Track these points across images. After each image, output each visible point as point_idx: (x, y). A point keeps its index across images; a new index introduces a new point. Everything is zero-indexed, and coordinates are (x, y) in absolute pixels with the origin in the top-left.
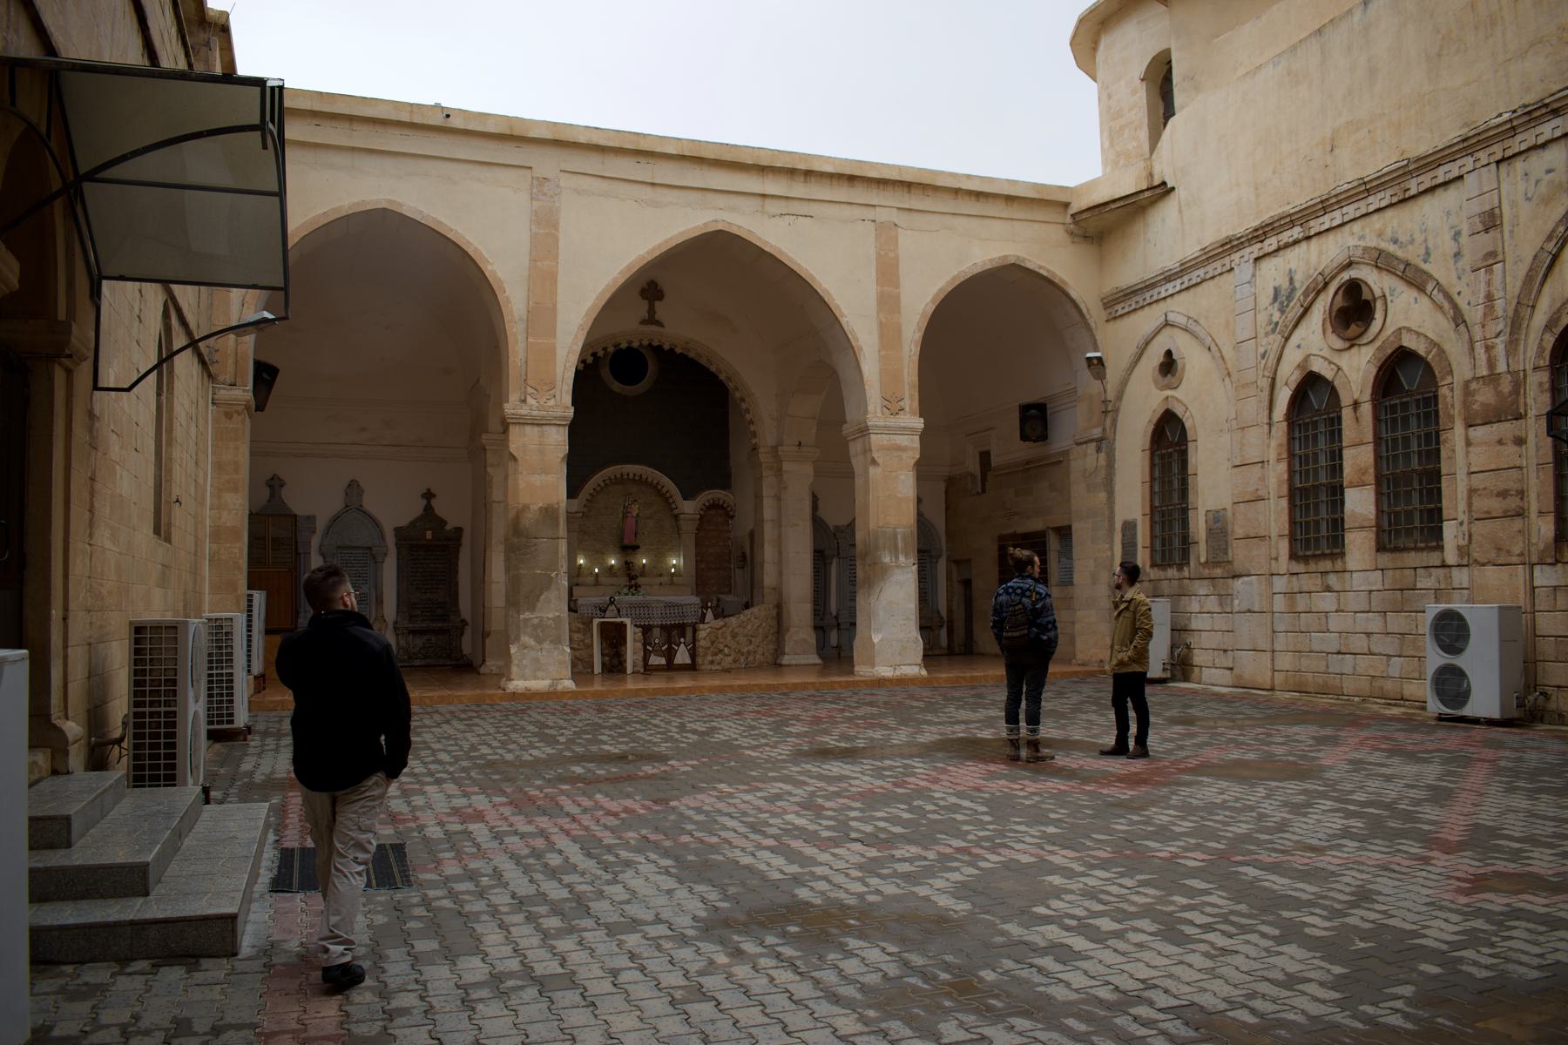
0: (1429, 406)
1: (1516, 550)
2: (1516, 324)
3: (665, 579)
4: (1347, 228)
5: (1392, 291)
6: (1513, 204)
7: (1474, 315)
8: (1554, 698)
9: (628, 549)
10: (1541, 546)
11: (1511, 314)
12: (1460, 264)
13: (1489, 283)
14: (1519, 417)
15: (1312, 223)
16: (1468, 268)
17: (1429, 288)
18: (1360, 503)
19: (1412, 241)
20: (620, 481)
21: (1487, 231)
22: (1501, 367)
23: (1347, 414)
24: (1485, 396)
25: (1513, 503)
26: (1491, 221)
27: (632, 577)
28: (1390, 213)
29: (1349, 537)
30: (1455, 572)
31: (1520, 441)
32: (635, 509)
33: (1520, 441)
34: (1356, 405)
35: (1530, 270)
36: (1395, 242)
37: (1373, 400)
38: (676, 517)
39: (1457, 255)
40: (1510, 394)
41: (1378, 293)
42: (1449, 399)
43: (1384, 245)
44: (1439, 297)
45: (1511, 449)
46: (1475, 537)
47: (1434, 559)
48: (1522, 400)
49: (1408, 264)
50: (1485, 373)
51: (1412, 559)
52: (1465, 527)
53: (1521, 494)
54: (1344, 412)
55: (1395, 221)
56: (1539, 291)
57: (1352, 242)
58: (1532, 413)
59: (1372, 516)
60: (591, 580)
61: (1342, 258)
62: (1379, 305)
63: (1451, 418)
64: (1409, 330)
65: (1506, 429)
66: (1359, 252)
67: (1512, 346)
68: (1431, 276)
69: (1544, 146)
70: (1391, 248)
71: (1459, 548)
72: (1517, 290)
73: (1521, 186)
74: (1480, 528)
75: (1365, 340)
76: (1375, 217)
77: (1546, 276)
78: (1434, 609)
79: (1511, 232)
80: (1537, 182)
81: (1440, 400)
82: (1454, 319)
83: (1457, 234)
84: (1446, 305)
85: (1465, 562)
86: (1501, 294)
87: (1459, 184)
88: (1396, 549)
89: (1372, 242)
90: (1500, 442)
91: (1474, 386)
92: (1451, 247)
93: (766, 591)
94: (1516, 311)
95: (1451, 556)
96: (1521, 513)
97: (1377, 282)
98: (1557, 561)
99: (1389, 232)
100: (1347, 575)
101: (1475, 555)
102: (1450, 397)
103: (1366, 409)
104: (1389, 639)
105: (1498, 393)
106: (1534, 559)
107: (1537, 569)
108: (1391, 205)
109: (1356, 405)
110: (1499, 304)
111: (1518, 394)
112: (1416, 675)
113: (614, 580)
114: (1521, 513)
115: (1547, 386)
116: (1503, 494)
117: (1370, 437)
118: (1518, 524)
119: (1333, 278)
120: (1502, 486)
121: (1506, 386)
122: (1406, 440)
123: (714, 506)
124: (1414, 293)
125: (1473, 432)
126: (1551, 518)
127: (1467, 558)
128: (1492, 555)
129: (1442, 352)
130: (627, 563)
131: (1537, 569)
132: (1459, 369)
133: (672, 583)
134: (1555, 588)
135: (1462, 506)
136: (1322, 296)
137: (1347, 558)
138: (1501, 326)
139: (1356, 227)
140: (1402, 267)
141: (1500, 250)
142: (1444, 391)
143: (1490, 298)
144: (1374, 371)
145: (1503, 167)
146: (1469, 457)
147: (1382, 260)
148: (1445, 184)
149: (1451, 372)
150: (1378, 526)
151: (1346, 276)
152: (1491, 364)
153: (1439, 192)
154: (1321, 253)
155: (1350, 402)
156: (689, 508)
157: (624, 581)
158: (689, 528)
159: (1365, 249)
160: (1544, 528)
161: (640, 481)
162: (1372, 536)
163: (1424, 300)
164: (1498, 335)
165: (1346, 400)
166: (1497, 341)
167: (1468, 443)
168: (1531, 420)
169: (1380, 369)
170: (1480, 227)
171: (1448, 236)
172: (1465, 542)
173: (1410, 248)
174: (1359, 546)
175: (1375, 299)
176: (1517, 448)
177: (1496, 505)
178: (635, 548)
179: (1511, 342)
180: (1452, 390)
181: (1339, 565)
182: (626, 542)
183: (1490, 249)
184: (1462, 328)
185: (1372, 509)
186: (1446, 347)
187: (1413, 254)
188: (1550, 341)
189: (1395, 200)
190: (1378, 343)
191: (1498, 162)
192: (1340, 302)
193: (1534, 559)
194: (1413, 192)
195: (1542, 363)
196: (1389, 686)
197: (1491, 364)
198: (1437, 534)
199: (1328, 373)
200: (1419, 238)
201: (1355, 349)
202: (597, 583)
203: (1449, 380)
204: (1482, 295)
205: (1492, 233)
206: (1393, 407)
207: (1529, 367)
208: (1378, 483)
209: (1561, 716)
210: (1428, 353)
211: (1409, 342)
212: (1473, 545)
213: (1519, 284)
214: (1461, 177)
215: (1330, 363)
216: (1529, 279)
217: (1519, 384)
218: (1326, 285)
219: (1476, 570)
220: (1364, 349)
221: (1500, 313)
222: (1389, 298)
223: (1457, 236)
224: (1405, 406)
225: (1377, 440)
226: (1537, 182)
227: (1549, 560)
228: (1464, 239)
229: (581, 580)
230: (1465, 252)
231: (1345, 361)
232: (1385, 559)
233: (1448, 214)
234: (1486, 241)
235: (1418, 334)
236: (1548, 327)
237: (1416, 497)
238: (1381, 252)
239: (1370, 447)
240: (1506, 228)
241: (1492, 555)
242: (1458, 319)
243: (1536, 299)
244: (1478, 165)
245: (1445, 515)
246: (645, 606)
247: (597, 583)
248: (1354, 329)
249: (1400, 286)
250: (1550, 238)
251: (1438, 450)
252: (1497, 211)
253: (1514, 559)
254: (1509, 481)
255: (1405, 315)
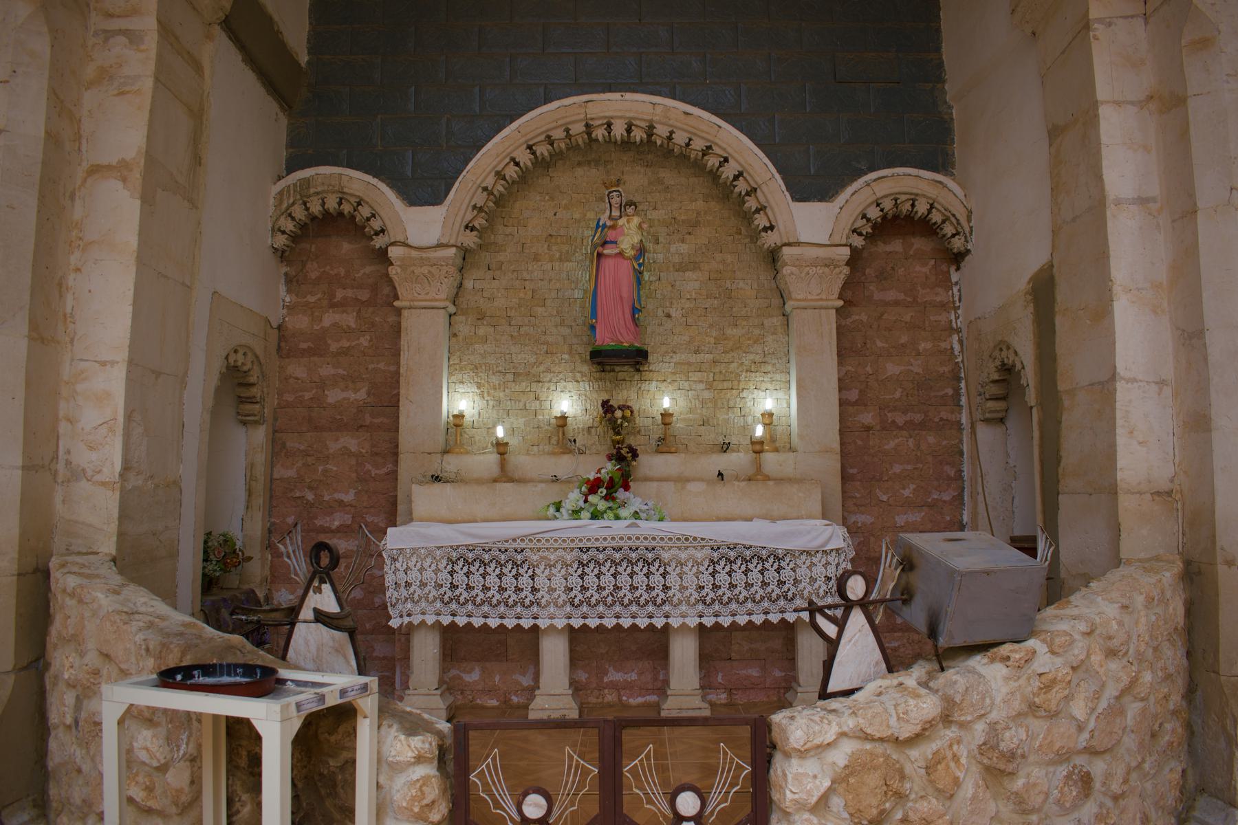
3: (737, 460)
9: (617, 361)
20: (589, 148)
27: (619, 461)
32: (629, 236)
38: (773, 257)
60: (492, 458)
93: (1126, 503)
113: (564, 465)
123: (896, 224)
130: (607, 407)
133: (757, 475)
156: (815, 227)
157: (599, 466)
158: (815, 292)
161: (649, 148)
178: (637, 358)
182: (604, 339)
202: (505, 475)
229: (452, 464)
246: (646, 558)
247: (505, 475)
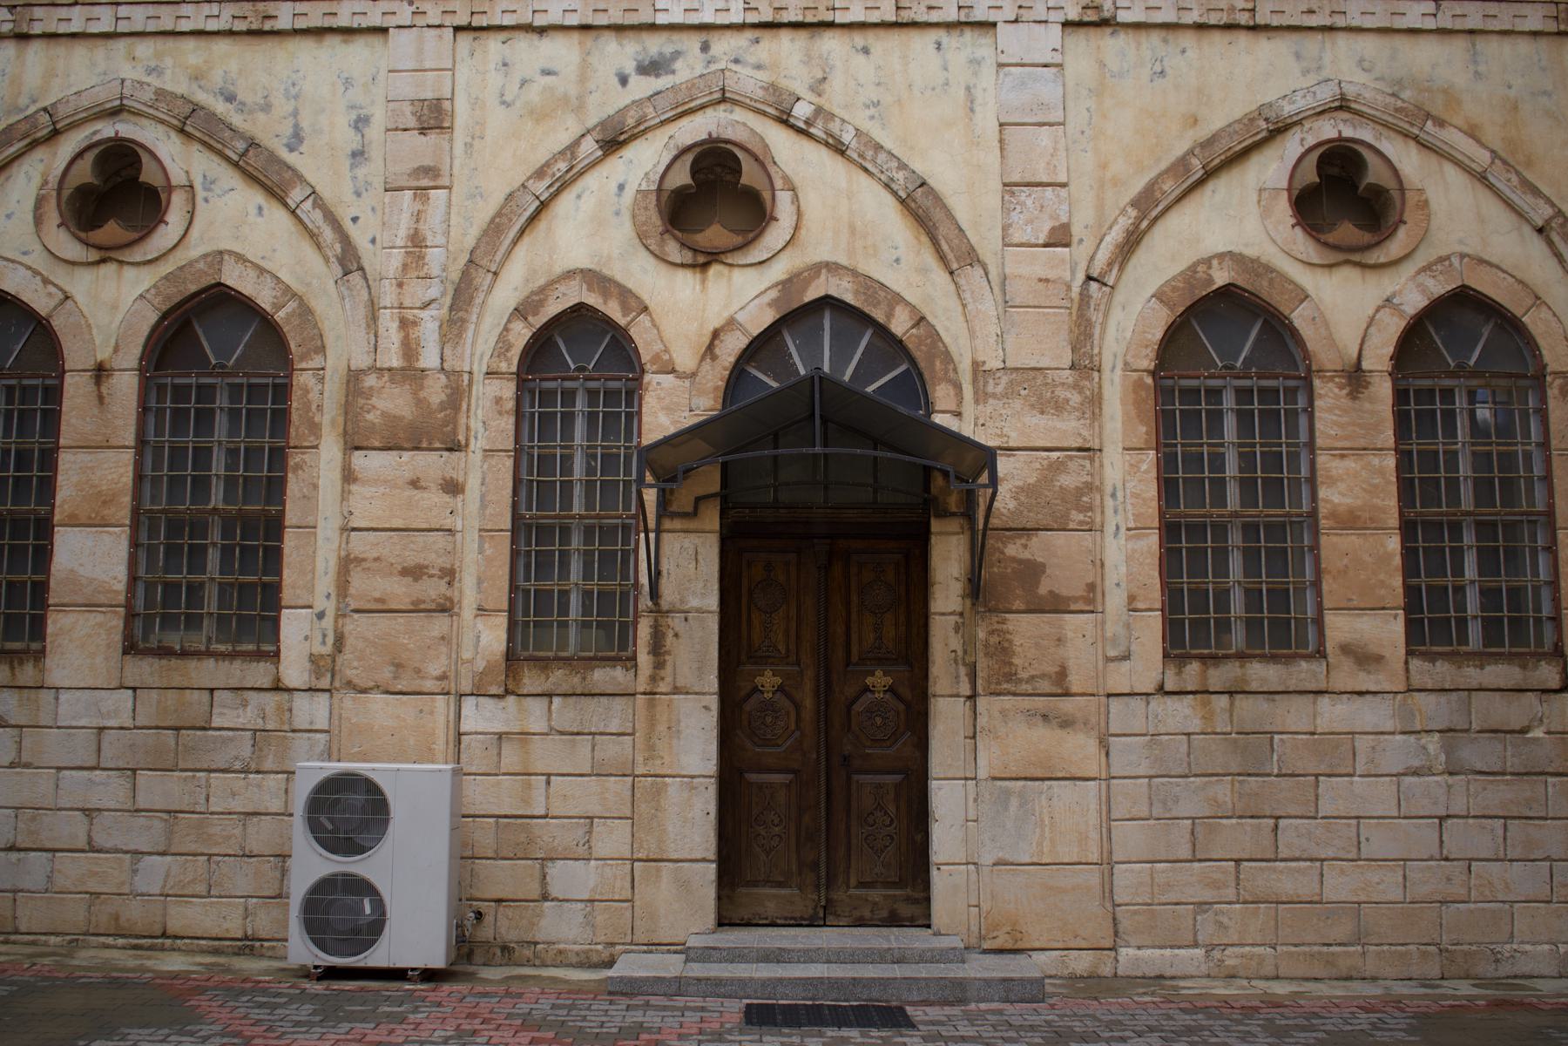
0: (269, 404)
1: (435, 669)
2: (463, 295)
4: (121, 44)
5: (209, 184)
6: (476, 103)
7: (384, 261)
8: (489, 919)
10: (480, 665)
11: (455, 276)
12: (361, 172)
13: (418, 217)
14: (454, 447)
15: (38, 12)
16: (378, 183)
17: (295, 195)
18: (91, 557)
19: (267, 107)
21: (423, 131)
22: (429, 358)
23: (76, 388)
24: (391, 402)
25: (432, 589)
26: (433, 118)
28: (222, 46)
29: (56, 623)
30: (300, 701)
31: (453, 488)
33: (453, 488)
34: (101, 372)
35: (499, 214)
36: (230, 98)
37: (141, 370)
39: (358, 155)
40: (443, 407)
41: (177, 177)
42: (314, 396)
43: (201, 97)
44: (315, 218)
45: (435, 498)
46: (350, 642)
47: (259, 673)
48: (462, 421)
49: (253, 144)
50: (396, 362)
51: (207, 672)
52: (328, 622)
53: (450, 575)
54: (69, 379)
55: (228, 60)
56: (509, 252)
57: (129, 72)
58: (477, 445)
59: (120, 586)
61: (106, 95)
62: (178, 201)
63: (315, 428)
64: (240, 258)
65: (431, 464)
66: (148, 96)
67: (453, 327)
68: (301, 178)
69: (542, 31)
70: (220, 107)
71: (314, 659)
72: (470, 242)
73: (495, 80)
74: (358, 627)
75: (137, 254)
76: (190, 44)
77: (522, 232)
78: (313, 770)
79: (469, 146)
80: (524, 83)
81: (296, 394)
82: (342, 261)
83: (360, 123)
84: (328, 234)
85: (325, 683)
86: (440, 240)
87: (376, 40)
88: (164, 652)
89: (176, 83)
90: (415, 484)
91: (370, 381)
92: (350, 140)
94: (465, 274)
95: (294, 670)
96: (446, 608)
97: (172, 155)
98: (508, 692)
99: (217, 78)
100: (46, 696)
101: (350, 673)
102: (318, 391)
103: (125, 385)
104: (141, 821)
105: (419, 402)
106: (466, 686)
107: (469, 704)
108: (231, 33)
109: (101, 372)
110: (435, 257)
111: (457, 409)
112: (201, 888)
114: (446, 608)
115: (511, 405)
116: (415, 572)
117: (129, 437)
118: (440, 624)
119: (73, 126)
120: (412, 559)
121: (435, 392)
122: (202, 456)
124: (258, 197)
125: (358, 459)
126: (502, 621)
127: (328, 673)
128: (386, 674)
129: (305, 311)
131: (469, 704)
132: (341, 341)
134: (500, 736)
135: (325, 583)
136: (40, 153)
137: (51, 661)
138: (434, 291)
139: (144, 48)
140: (241, 146)
141: (445, 169)
142: (303, 379)
143: (417, 241)
144: (153, 317)
145: (465, 39)
146: (338, 505)
147: (194, 124)
148: (348, 32)
149: (322, 349)
150: (129, 606)
151: (106, 130)
152: (410, 350)
153: (333, 41)
154: (50, 74)
155: (90, 364)
159: (160, 93)
160: (489, 638)
162: (118, 623)
163: (278, 215)
164: (425, 306)
165: (76, 356)
166: (425, 314)
167: (349, 476)
168: (475, 455)
169: (164, 317)
170: (412, 123)
171: (343, 121)
172: (328, 649)
173: (261, 116)
174: (81, 643)
175: (170, 188)
176: (447, 498)
177: (399, 590)
179: (451, 322)
180: (322, 380)
181: (27, 673)
183: (427, 162)
184: (356, 278)
185: (121, 572)
186: (319, 305)
187: (270, 131)
188: (521, 334)
189: (240, 26)
190: (167, 267)
191: (457, 29)
192: (85, 172)
193: (466, 686)
194: (284, 23)
195: (503, 367)
196: (135, 913)
197: (410, 350)
198: (272, 627)
199: (41, 302)
200: (282, 107)
201: (109, 269)
203: (317, 362)
204: (402, 233)
205: (433, 137)
206: (181, 393)
207: (479, 369)
208: (135, 526)
209: (505, 949)
210: (279, 307)
211: (236, 278)
212: (347, 655)
213: (474, 233)
214: (383, 31)
215: (46, 281)
216: (494, 228)
217: (457, 395)
218: (55, 133)
219: (348, 700)
220: (129, 273)
221: (435, 270)
222: (200, 194)
223: (360, 123)
224: (206, 393)
225: (141, 443)
226: (524, 83)
227: (494, 690)
228: (375, 132)
230: (375, 153)
231: (81, 284)
232: (144, 670)
233: (348, 83)
234: (421, 148)
235: (262, 271)
236: (520, 312)
237: (213, 558)
238: (196, 108)
239: (128, 457)
240: (460, 136)
241: (386, 674)
242: (349, 262)
243: (502, 264)
244: (420, 21)
245: (287, 595)
248: (111, 231)
249: (228, 178)
250: (540, 173)
251: (282, 481)
252: (447, 105)
253: (429, 685)
254: (429, 550)
255: (224, 228)
